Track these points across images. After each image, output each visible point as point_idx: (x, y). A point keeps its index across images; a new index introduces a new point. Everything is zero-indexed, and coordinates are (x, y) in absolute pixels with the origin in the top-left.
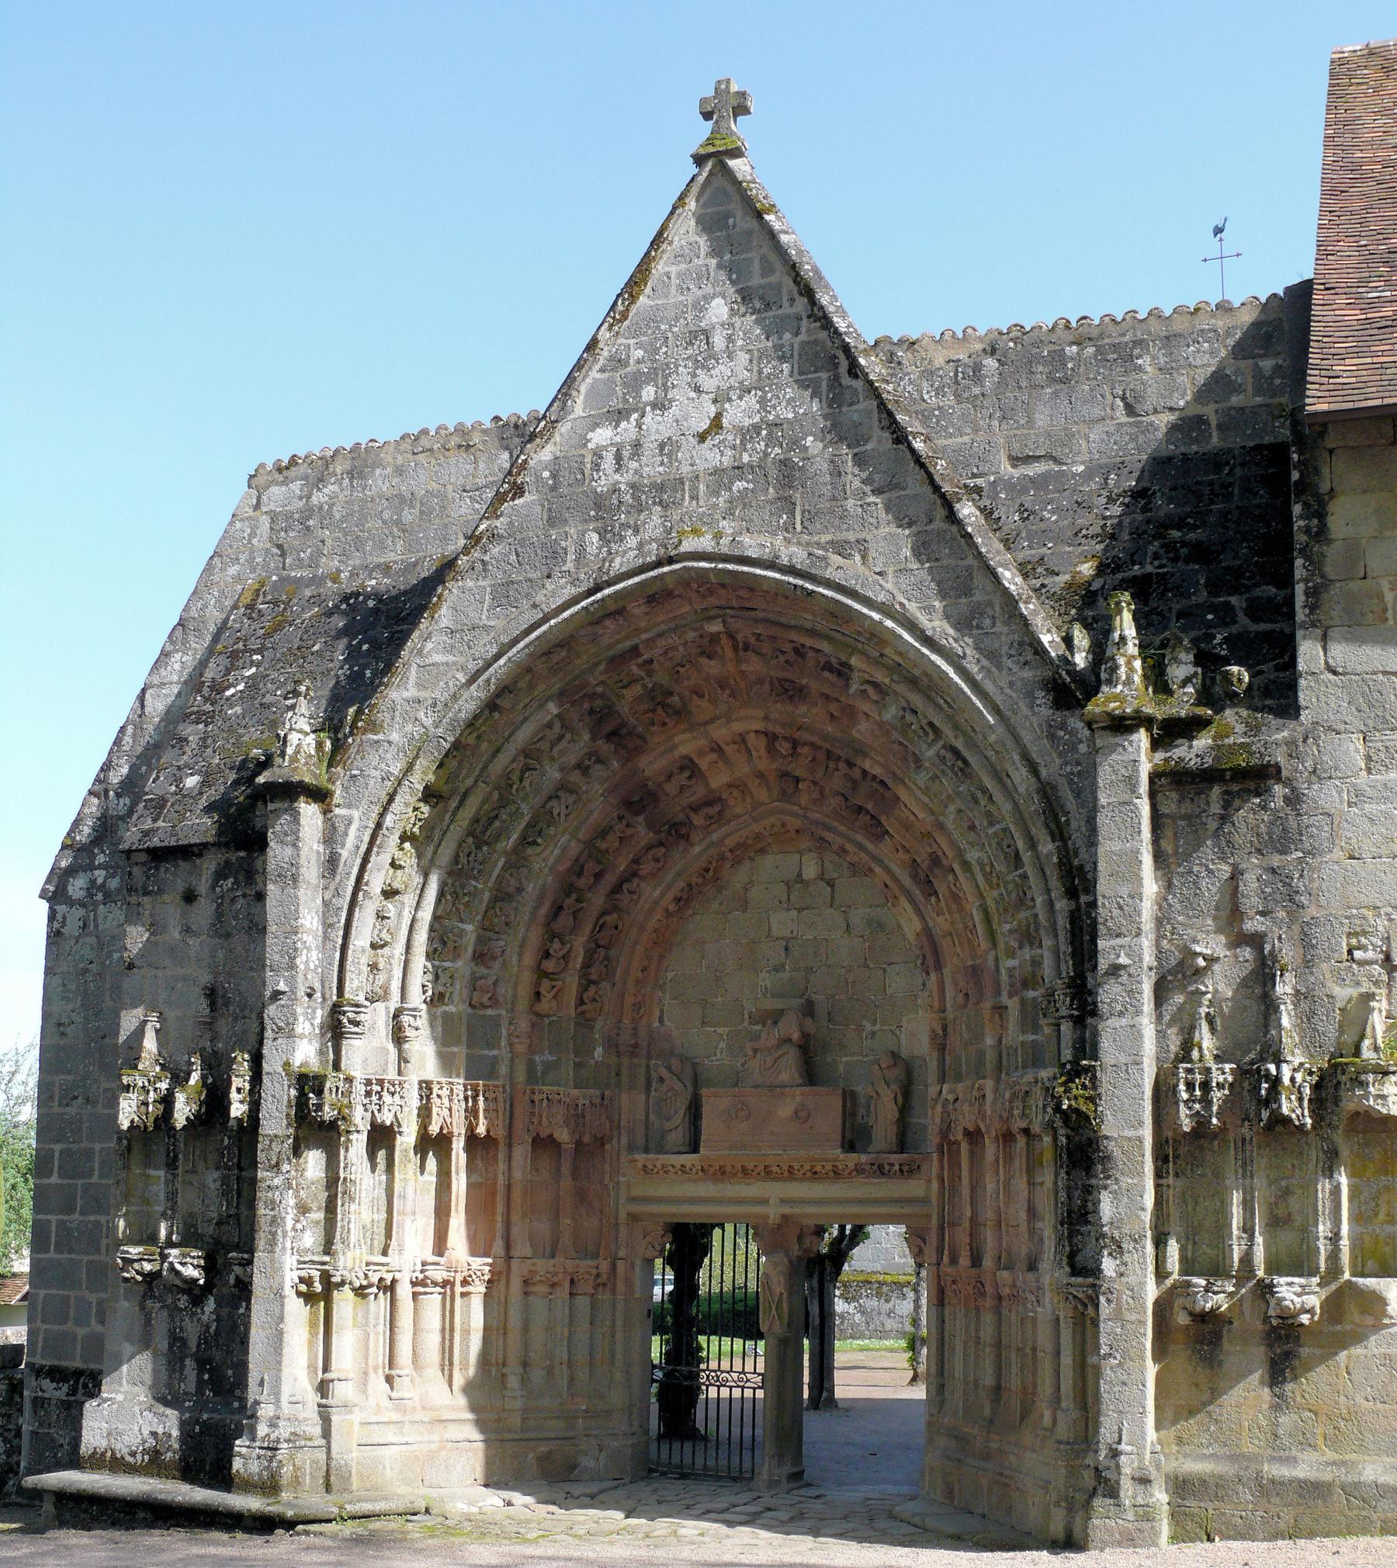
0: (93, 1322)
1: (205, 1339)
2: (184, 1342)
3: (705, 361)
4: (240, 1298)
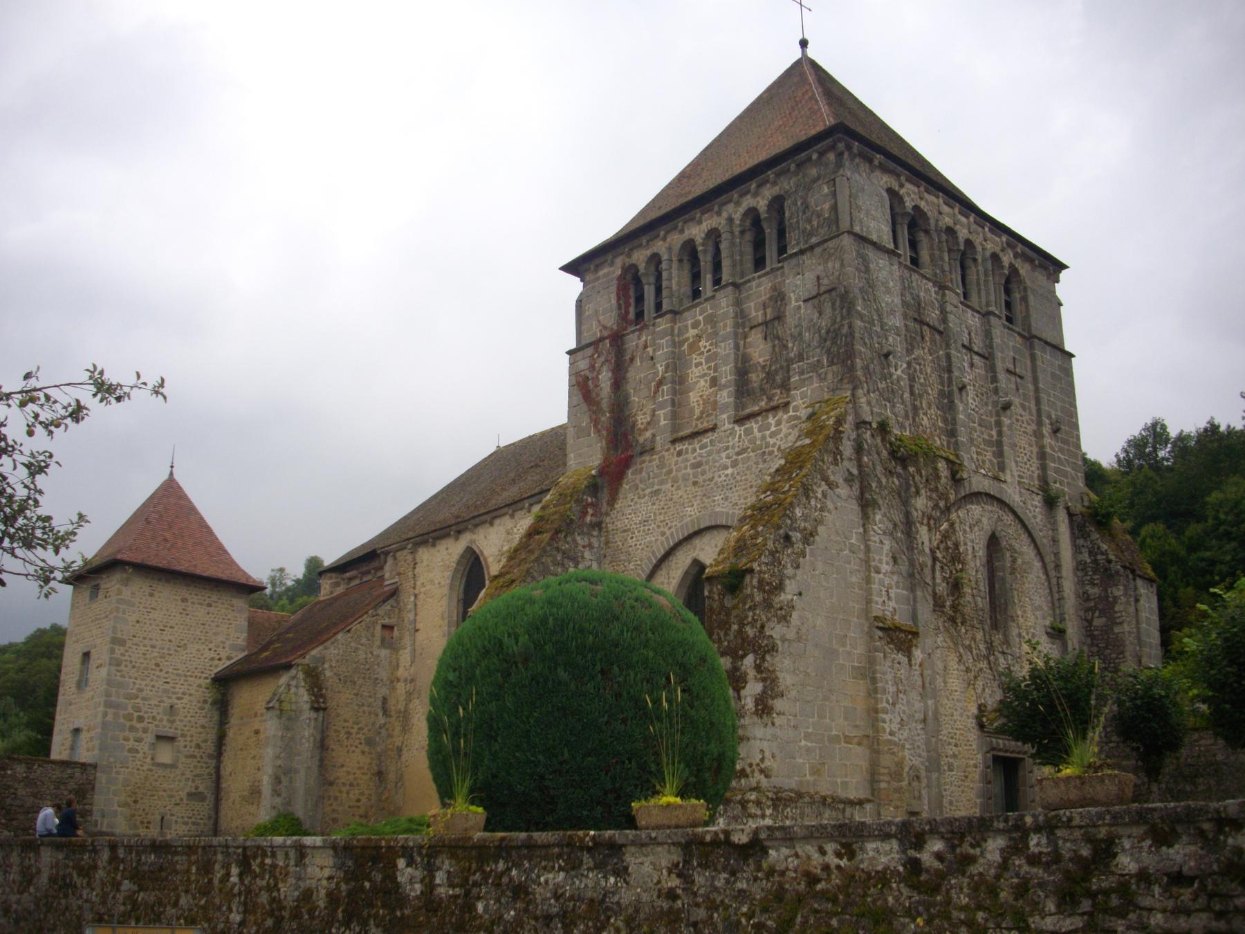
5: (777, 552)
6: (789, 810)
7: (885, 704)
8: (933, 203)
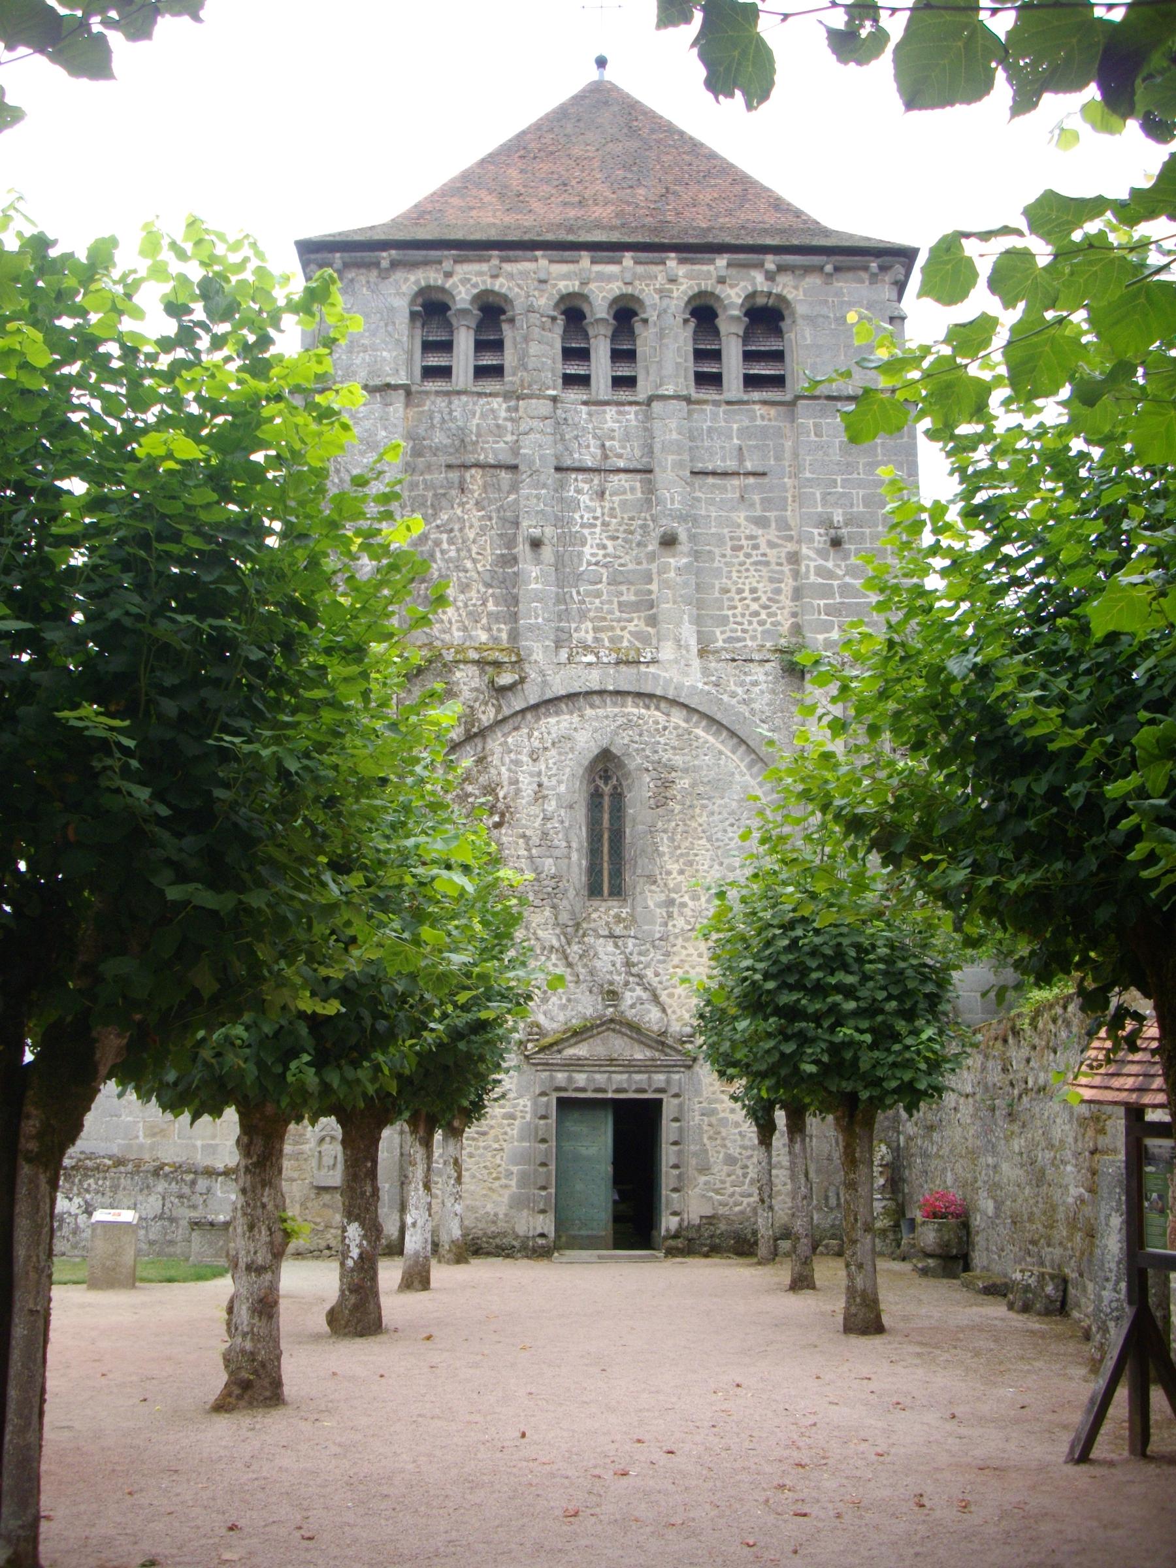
6: (91, 1181)
8: (524, 274)
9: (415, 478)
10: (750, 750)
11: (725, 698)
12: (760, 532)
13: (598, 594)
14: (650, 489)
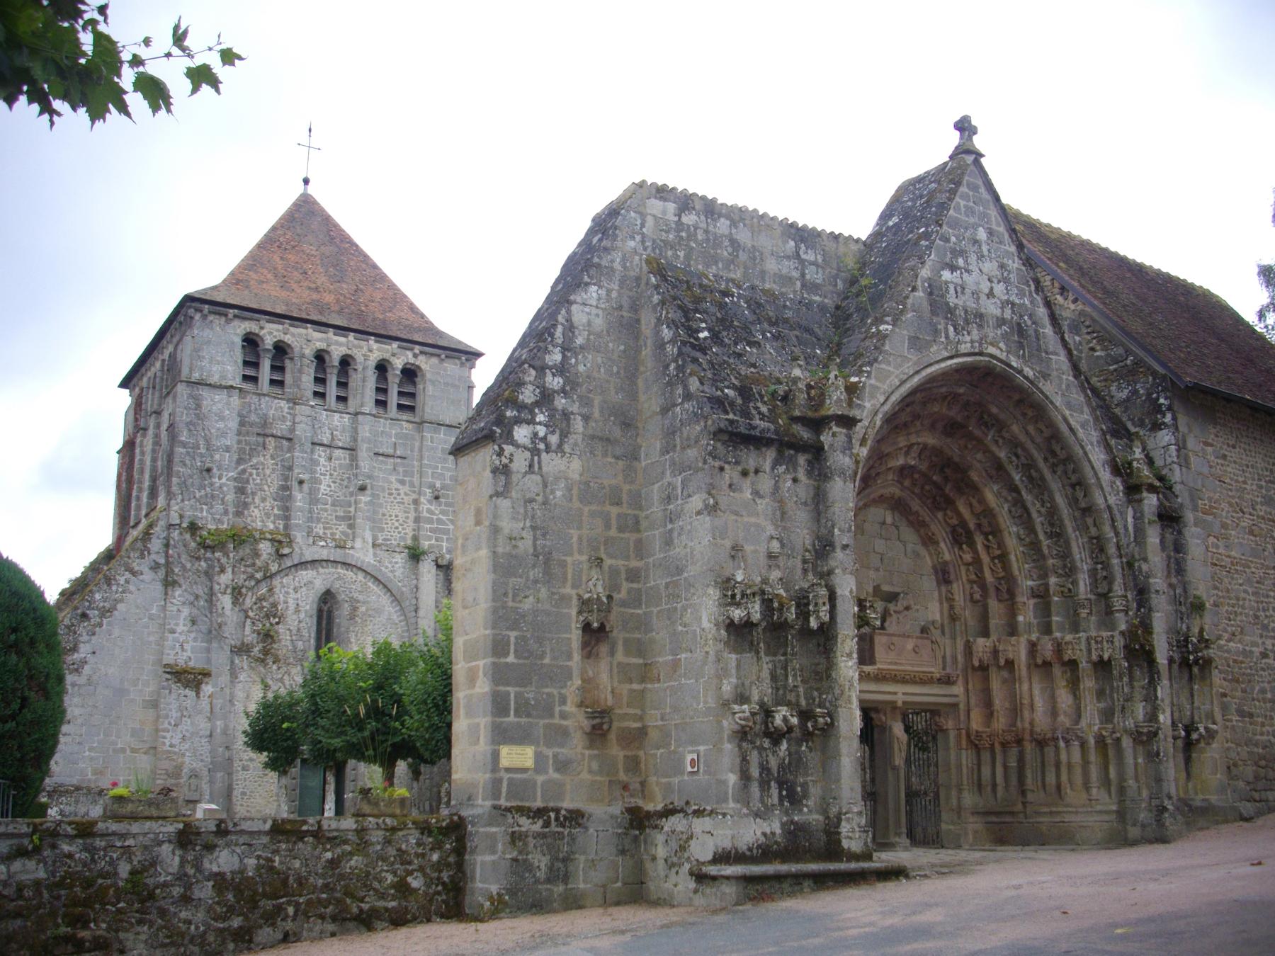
0: (551, 771)
1: (781, 766)
2: (769, 770)
3: (981, 257)
4: (802, 741)
5: (73, 625)
7: (166, 725)
8: (300, 335)
9: (241, 438)
10: (392, 595)
11: (383, 569)
12: (401, 487)
13: (326, 510)
14: (354, 458)
